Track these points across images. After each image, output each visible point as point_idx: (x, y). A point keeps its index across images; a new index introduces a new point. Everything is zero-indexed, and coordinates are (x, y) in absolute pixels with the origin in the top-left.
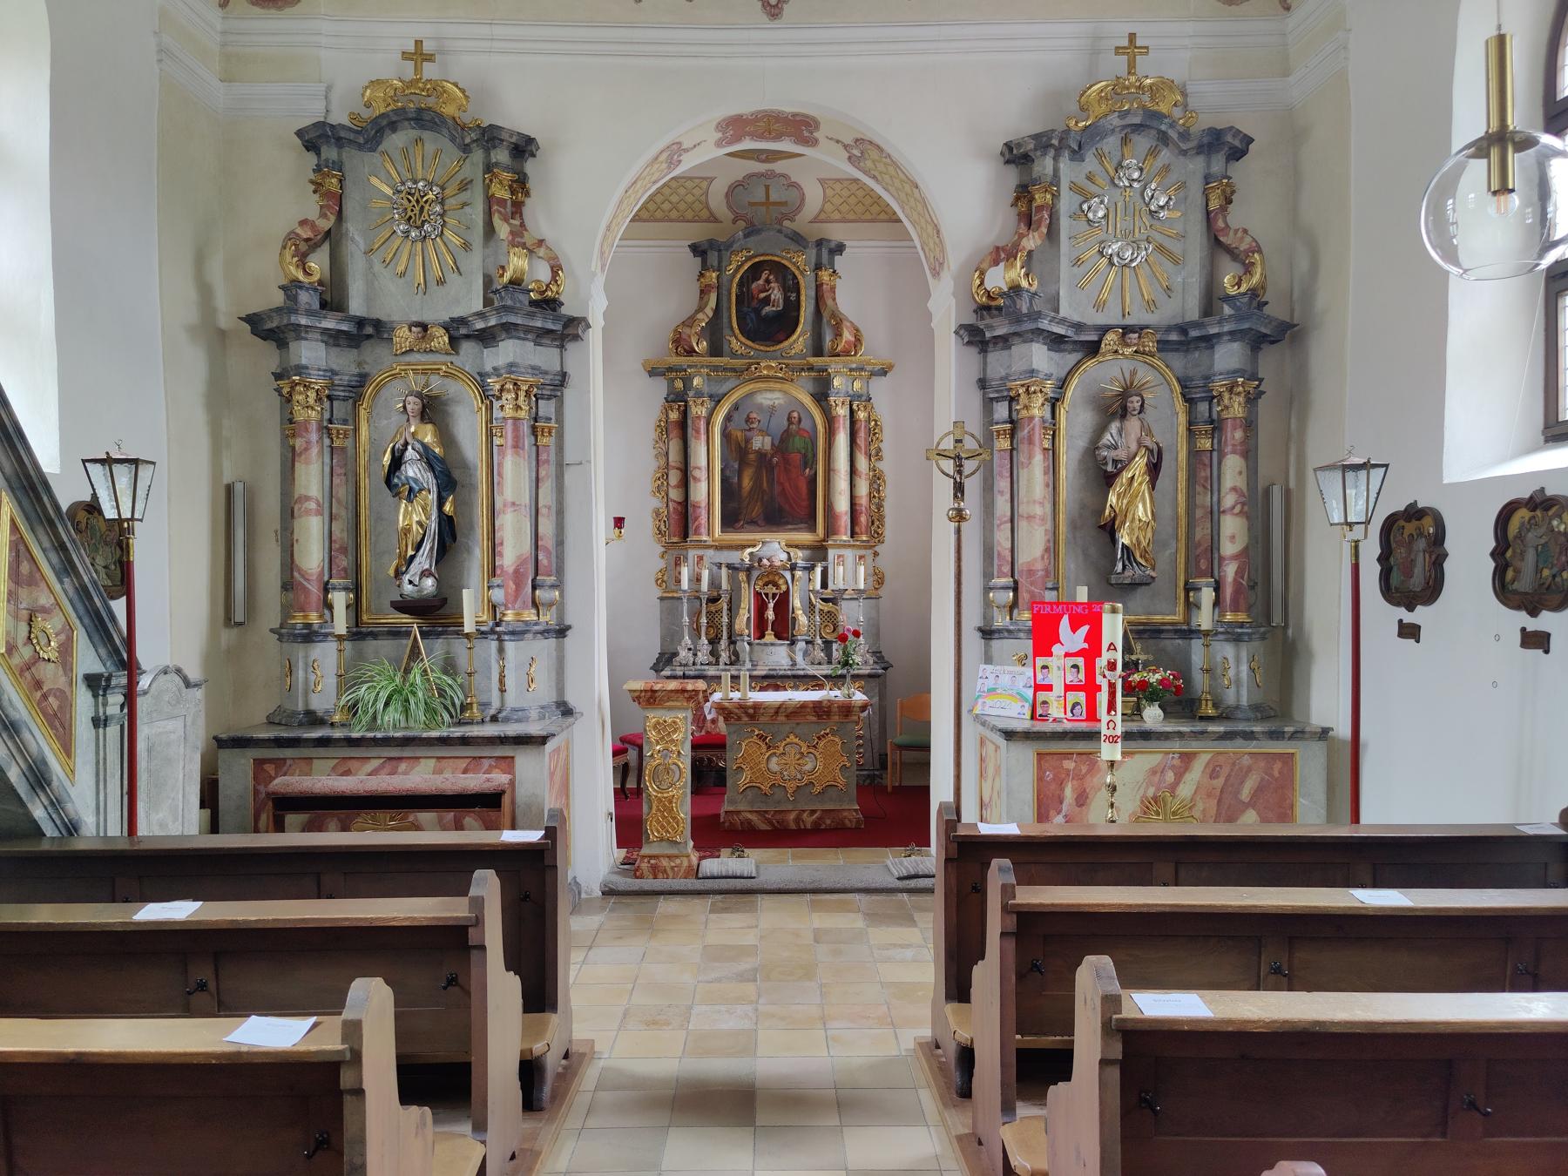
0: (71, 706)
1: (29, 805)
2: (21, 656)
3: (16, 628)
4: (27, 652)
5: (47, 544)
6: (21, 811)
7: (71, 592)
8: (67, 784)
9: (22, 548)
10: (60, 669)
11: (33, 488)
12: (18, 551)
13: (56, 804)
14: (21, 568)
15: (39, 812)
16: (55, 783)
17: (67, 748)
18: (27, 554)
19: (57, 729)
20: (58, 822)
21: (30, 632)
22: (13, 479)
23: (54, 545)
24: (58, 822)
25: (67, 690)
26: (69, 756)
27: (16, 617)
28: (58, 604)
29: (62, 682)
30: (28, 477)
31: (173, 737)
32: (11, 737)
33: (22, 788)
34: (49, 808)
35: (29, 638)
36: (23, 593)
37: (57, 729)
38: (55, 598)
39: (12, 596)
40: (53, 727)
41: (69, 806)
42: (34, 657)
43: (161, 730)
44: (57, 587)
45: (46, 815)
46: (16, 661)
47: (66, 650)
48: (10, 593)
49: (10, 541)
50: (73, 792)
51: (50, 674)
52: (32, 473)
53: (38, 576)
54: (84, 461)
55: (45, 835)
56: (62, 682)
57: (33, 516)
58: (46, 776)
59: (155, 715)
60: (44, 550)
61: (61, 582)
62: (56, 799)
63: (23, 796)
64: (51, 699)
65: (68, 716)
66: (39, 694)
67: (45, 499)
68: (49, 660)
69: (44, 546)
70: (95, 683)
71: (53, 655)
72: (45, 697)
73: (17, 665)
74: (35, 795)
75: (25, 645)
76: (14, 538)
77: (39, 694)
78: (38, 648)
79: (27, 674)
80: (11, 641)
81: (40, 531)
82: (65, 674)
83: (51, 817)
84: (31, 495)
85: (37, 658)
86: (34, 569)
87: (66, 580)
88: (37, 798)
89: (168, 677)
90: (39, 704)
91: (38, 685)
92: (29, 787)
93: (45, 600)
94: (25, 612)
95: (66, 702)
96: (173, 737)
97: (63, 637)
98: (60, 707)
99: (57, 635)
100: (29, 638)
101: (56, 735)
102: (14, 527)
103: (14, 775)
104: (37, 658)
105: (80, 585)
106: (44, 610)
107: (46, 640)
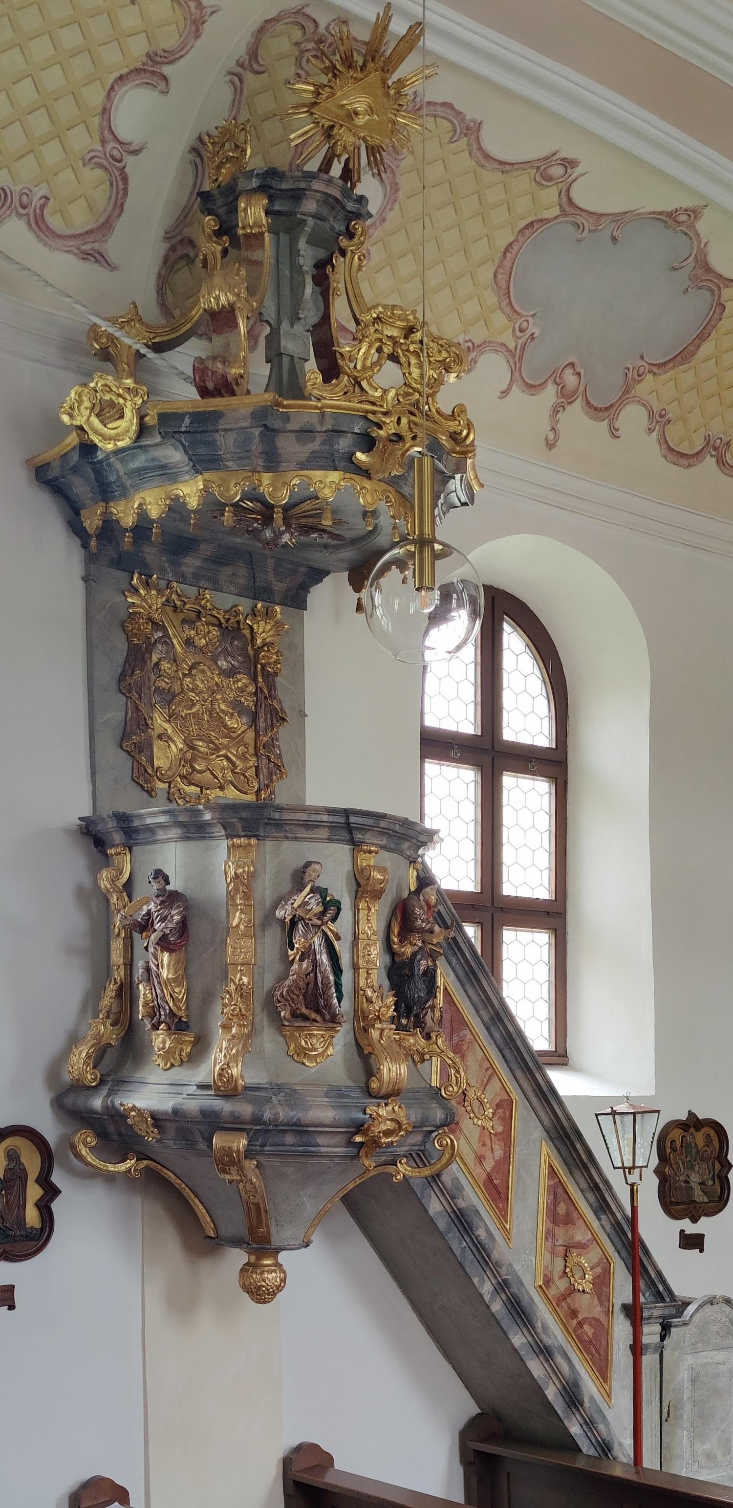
0: (608, 1333)
1: (566, 1422)
2: (558, 1288)
3: (553, 1262)
4: (561, 1285)
5: (584, 1185)
6: (561, 1424)
7: (608, 1227)
8: (603, 1406)
9: (560, 1190)
10: (596, 1300)
11: (568, 1137)
12: (555, 1195)
13: (589, 1424)
14: (558, 1209)
15: (575, 1429)
16: (587, 1404)
17: (603, 1371)
18: (566, 1196)
19: (593, 1356)
20: (593, 1440)
21: (566, 1266)
22: (552, 1130)
23: (590, 1187)
24: (593, 1440)
25: (603, 1319)
26: (605, 1381)
27: (553, 1253)
28: (595, 1239)
29: (597, 1311)
30: (562, 1127)
31: (721, 1368)
32: (547, 1361)
33: (559, 1406)
34: (584, 1427)
35: (564, 1272)
36: (560, 1231)
37: (593, 1356)
38: (592, 1234)
39: (550, 1235)
40: (589, 1352)
41: (601, 1427)
42: (569, 1288)
43: (709, 1360)
44: (595, 1224)
45: (582, 1432)
46: (552, 1292)
47: (602, 1282)
48: (548, 1232)
49: (548, 1186)
50: (610, 1415)
51: (588, 1306)
52: (565, 1124)
53: (575, 1214)
54: (597, 1115)
55: (581, 1451)
56: (597, 1311)
57: (570, 1160)
58: (579, 1397)
59: (700, 1345)
60: (582, 1191)
61: (599, 1219)
62: (589, 1418)
63: (559, 1412)
64: (586, 1327)
65: (604, 1343)
66: (575, 1322)
67: (578, 1146)
68: (583, 1291)
69: (582, 1187)
70: (633, 1312)
71: (588, 1287)
72: (580, 1324)
73: (553, 1296)
74: (571, 1412)
75: (561, 1277)
76: (552, 1183)
77: (575, 1322)
78: (572, 1280)
79: (563, 1304)
80: (549, 1275)
81: (578, 1174)
82: (601, 1304)
83: (587, 1434)
84: (568, 1143)
85: (572, 1291)
86: (572, 1208)
87: (603, 1217)
88: (573, 1416)
89: (716, 1308)
90: (575, 1331)
91: (574, 1314)
92: (565, 1405)
93: (581, 1236)
94: (561, 1248)
95: (603, 1331)
96: (721, 1368)
97: (598, 1270)
98: (595, 1334)
99: (592, 1268)
100: (564, 1272)
101: (591, 1360)
102: (552, 1172)
103: (551, 1392)
104: (572, 1291)
105: (615, 1221)
106: (581, 1246)
107: (581, 1273)
